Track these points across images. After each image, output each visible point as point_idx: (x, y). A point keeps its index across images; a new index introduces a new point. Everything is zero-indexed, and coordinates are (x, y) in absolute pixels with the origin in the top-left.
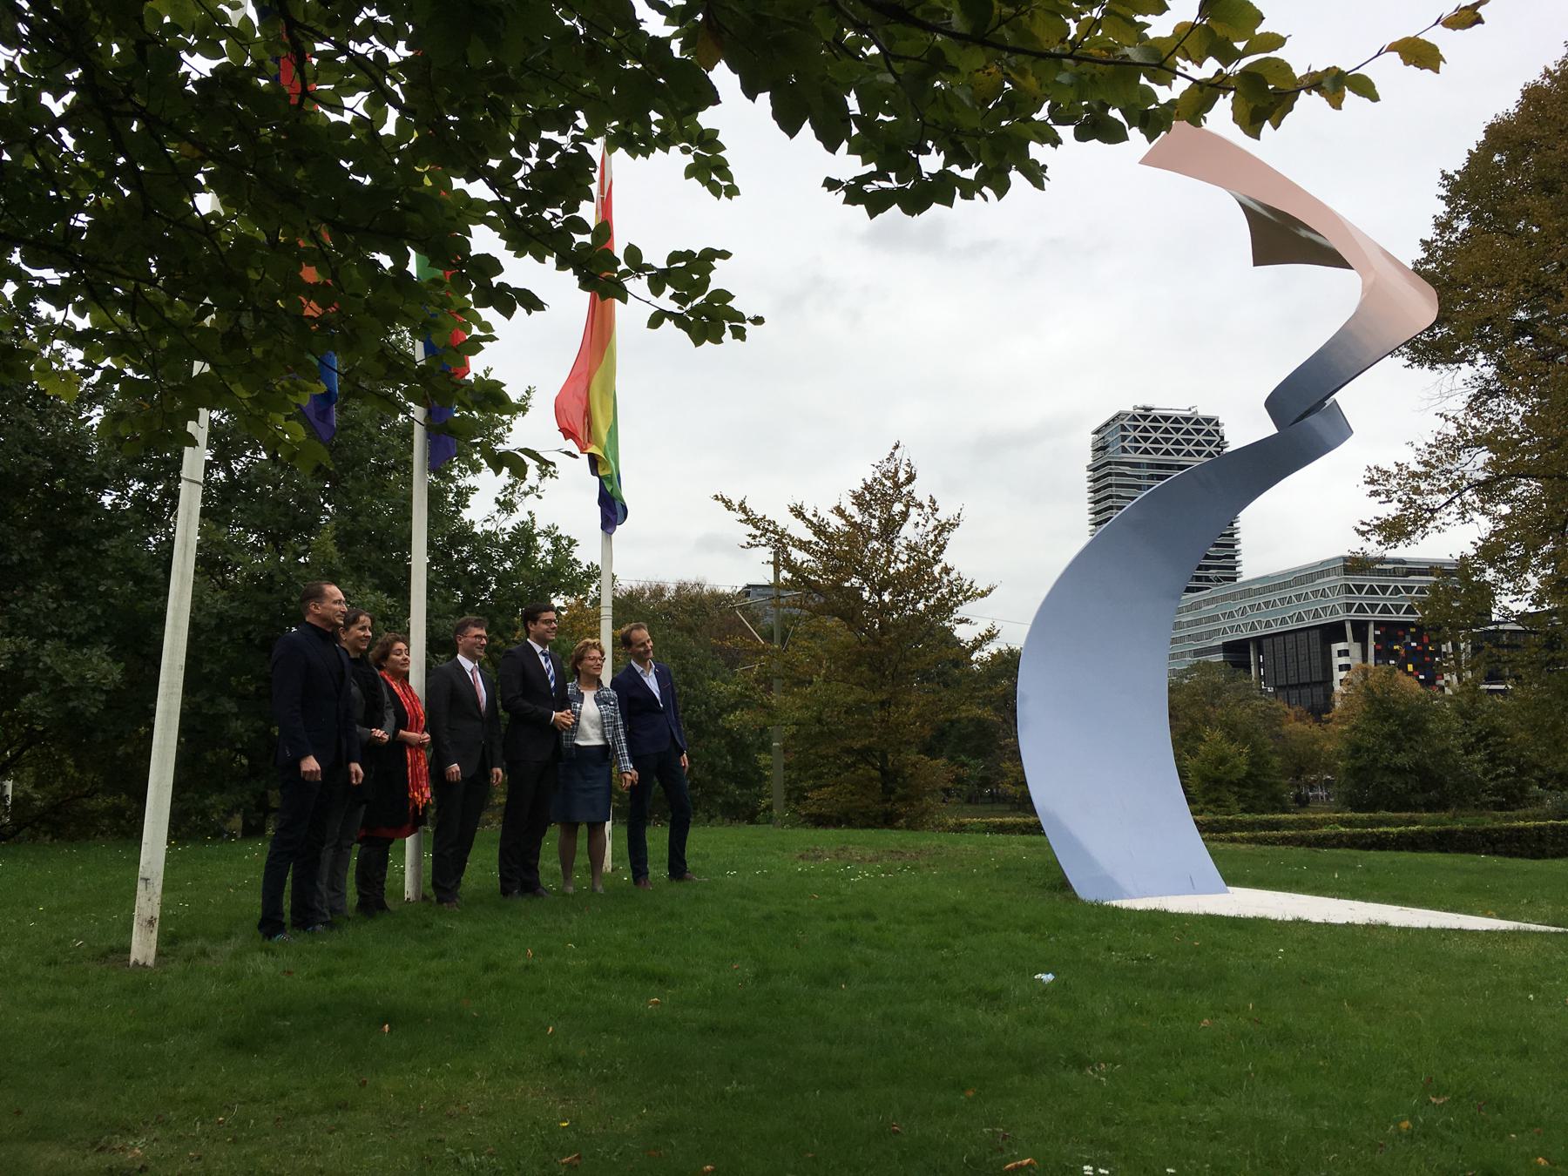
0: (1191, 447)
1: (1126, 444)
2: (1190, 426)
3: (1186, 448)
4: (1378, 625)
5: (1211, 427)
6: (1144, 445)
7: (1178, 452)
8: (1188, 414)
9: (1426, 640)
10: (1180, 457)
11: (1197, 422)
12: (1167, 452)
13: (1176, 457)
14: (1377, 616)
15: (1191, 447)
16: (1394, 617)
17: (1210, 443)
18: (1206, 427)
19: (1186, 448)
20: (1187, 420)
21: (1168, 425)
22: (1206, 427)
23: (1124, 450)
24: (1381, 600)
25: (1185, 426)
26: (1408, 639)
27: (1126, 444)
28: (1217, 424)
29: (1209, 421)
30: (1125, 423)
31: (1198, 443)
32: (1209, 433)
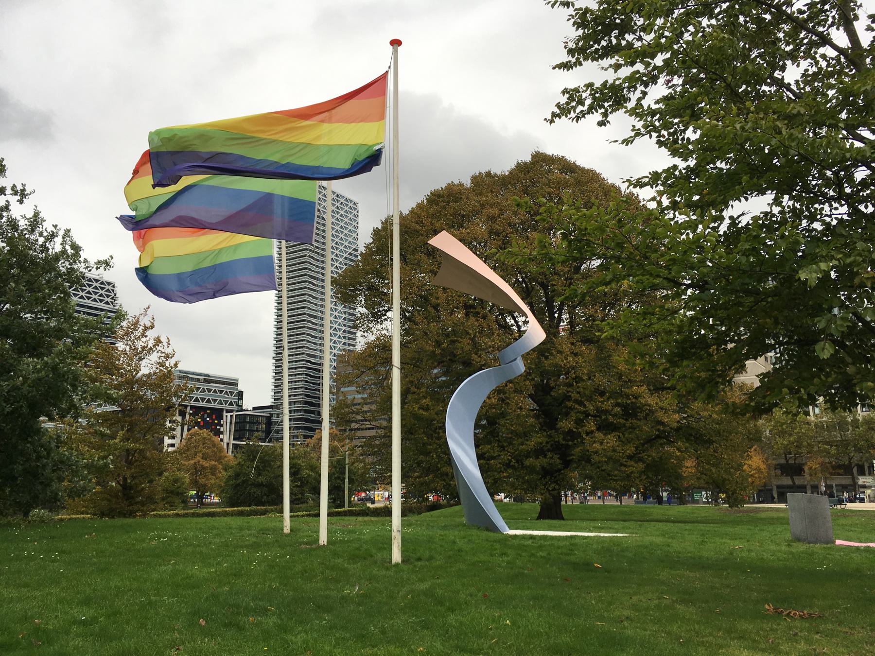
0: (96, 297)
2: (97, 285)
3: (94, 296)
4: (192, 407)
5: (110, 288)
7: (89, 298)
8: (97, 277)
9: (214, 417)
10: (89, 301)
11: (102, 283)
13: (87, 301)
14: (193, 403)
15: (96, 297)
16: (201, 404)
17: (108, 296)
18: (107, 287)
19: (94, 296)
20: (97, 281)
22: (107, 287)
24: (196, 394)
25: (95, 284)
26: (206, 416)
28: (114, 286)
29: (109, 284)
31: (101, 295)
32: (108, 291)
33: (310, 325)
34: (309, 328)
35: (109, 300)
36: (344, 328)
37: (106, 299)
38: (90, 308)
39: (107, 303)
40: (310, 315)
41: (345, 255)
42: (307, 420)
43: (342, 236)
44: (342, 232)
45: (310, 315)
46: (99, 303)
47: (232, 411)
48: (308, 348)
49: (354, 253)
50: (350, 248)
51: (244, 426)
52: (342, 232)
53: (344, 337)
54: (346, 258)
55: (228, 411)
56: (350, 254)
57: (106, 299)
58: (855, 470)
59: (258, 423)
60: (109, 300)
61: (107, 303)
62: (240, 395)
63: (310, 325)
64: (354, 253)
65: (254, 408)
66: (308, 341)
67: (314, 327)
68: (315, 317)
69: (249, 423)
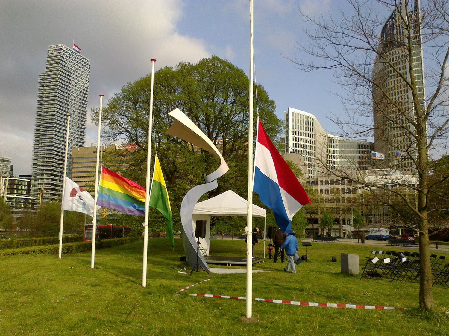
33: (57, 129)
34: (56, 131)
36: (77, 132)
40: (57, 124)
41: (80, 90)
42: (53, 185)
43: (79, 79)
44: (79, 77)
45: (57, 124)
47: (6, 177)
48: (55, 143)
49: (86, 89)
50: (84, 86)
51: (14, 186)
52: (79, 77)
53: (77, 138)
54: (81, 92)
55: (3, 177)
56: (83, 90)
58: (341, 222)
59: (22, 185)
62: (12, 168)
63: (57, 129)
64: (86, 89)
65: (20, 176)
66: (55, 139)
67: (59, 130)
68: (60, 125)
69: (16, 184)
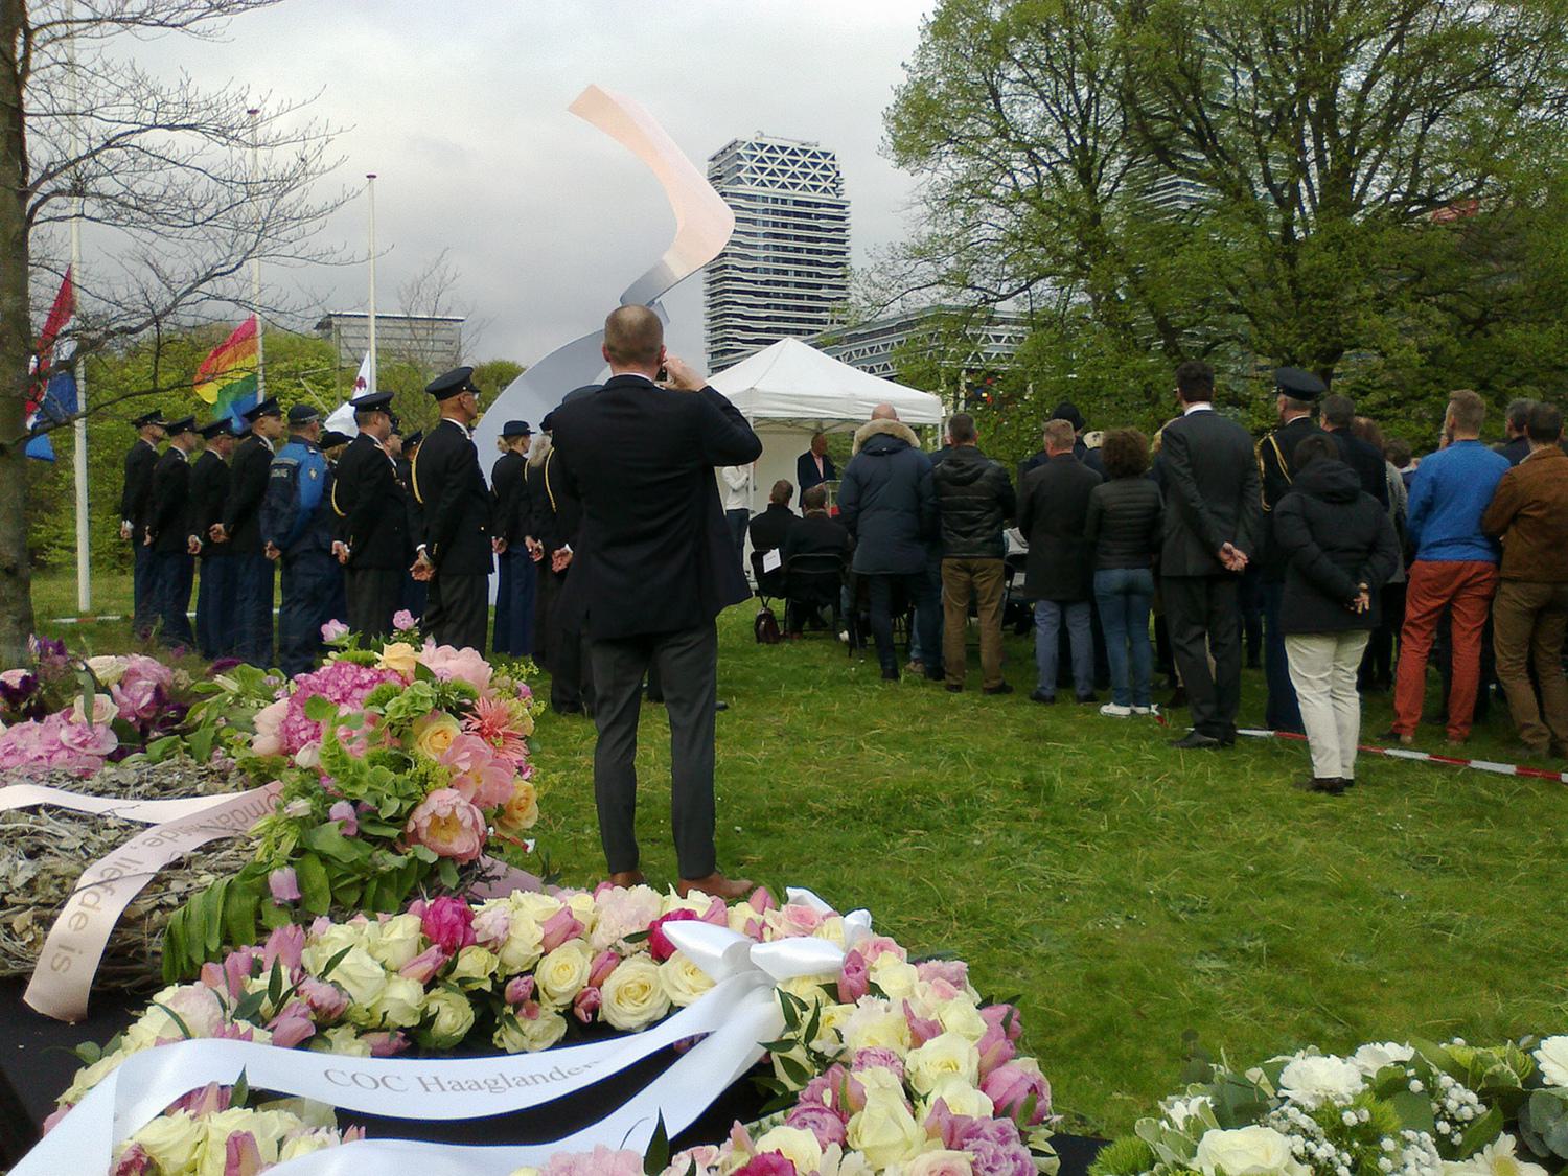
1: (741, 174)
5: (827, 162)
6: (760, 176)
7: (794, 185)
10: (796, 192)
12: (784, 186)
13: (791, 191)
17: (826, 177)
18: (823, 161)
19: (802, 181)
21: (785, 156)
22: (823, 161)
23: (740, 181)
27: (741, 174)
28: (833, 159)
29: (825, 154)
30: (741, 151)
32: (825, 168)
35: (827, 184)
37: (823, 184)
38: (796, 203)
39: (825, 190)
46: (813, 194)
57: (823, 184)
60: (827, 184)
61: (825, 190)
